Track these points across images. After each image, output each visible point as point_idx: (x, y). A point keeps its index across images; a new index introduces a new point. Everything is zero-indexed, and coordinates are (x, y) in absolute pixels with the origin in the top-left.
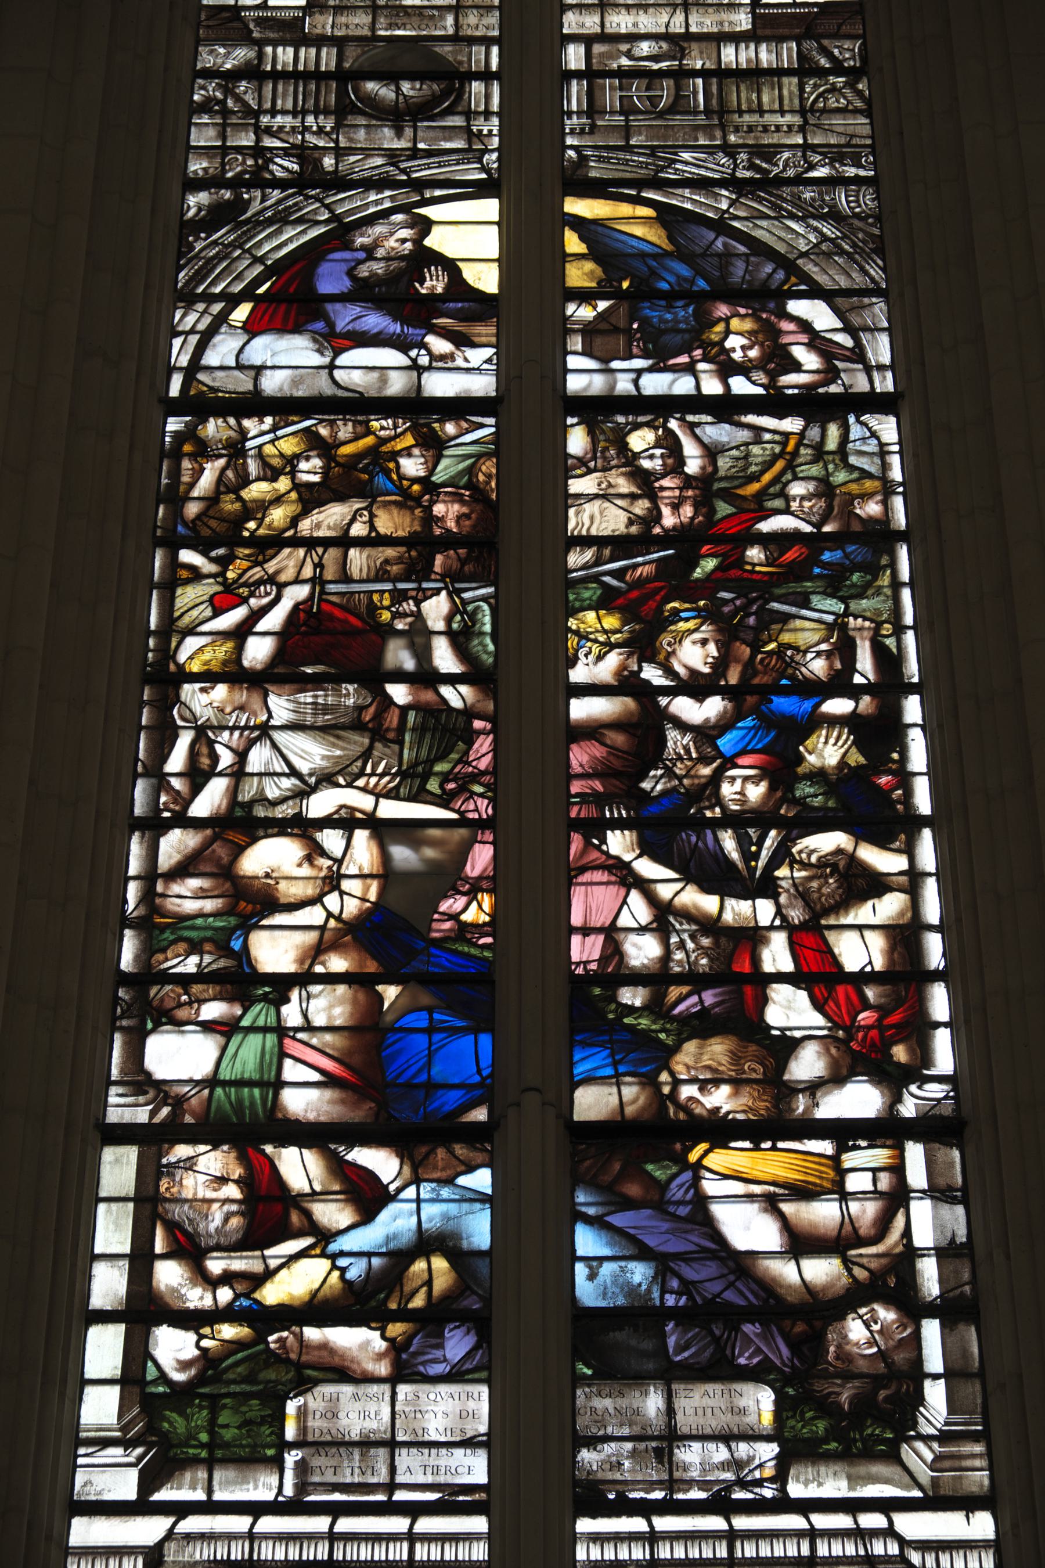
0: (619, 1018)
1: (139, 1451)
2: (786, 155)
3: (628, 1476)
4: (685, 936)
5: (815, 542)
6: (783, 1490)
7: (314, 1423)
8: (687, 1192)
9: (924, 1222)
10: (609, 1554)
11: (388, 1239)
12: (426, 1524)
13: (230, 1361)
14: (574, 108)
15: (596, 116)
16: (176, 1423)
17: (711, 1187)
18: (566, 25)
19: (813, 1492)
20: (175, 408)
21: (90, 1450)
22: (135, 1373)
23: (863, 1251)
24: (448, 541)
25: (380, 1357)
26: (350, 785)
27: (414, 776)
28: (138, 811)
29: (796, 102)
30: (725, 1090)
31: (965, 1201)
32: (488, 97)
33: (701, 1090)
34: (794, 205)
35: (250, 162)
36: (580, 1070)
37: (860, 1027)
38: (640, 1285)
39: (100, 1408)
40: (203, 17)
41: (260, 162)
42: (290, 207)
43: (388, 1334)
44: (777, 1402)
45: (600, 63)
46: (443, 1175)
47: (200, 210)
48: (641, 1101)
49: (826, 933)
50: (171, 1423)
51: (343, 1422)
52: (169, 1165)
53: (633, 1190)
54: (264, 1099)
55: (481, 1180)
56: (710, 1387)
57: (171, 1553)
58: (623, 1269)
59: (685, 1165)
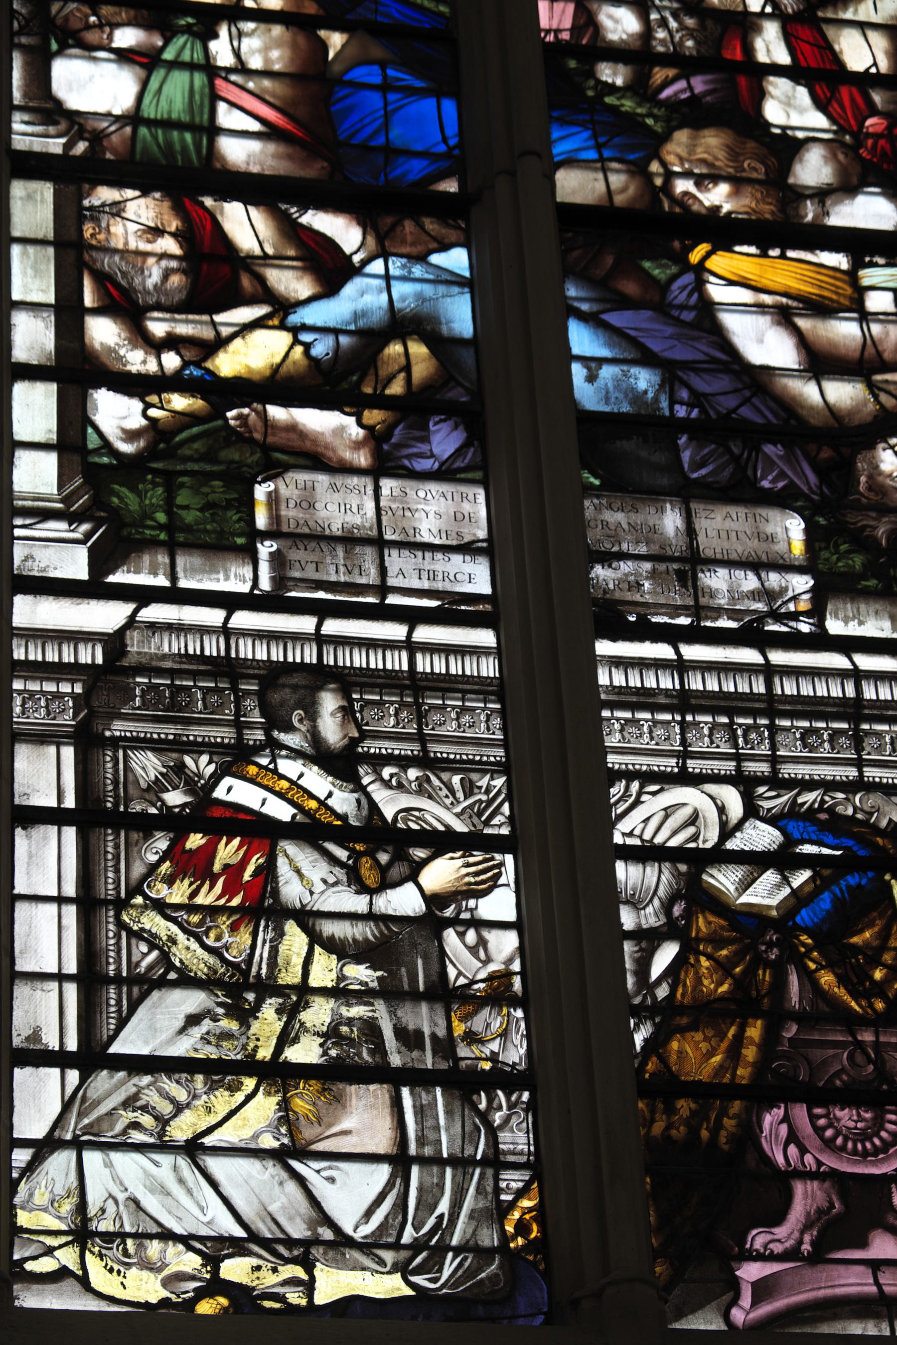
0: (600, 96)
3: (648, 598)
4: (667, 14)
6: (821, 624)
7: (289, 513)
8: (690, 295)
10: (635, 681)
11: (356, 316)
12: (425, 633)
13: (184, 435)
16: (127, 499)
17: (718, 292)
19: (853, 629)
21: (28, 521)
22: (73, 437)
25: (357, 445)
30: (724, 188)
33: (698, 184)
36: (560, 149)
37: (868, 135)
38: (646, 392)
44: (807, 531)
46: (414, 251)
48: (631, 191)
49: (824, 27)
50: (121, 499)
51: (322, 514)
52: (91, 208)
53: (630, 288)
54: (198, 145)
55: (457, 260)
56: (733, 510)
57: (135, 644)
58: (625, 374)
59: (686, 267)
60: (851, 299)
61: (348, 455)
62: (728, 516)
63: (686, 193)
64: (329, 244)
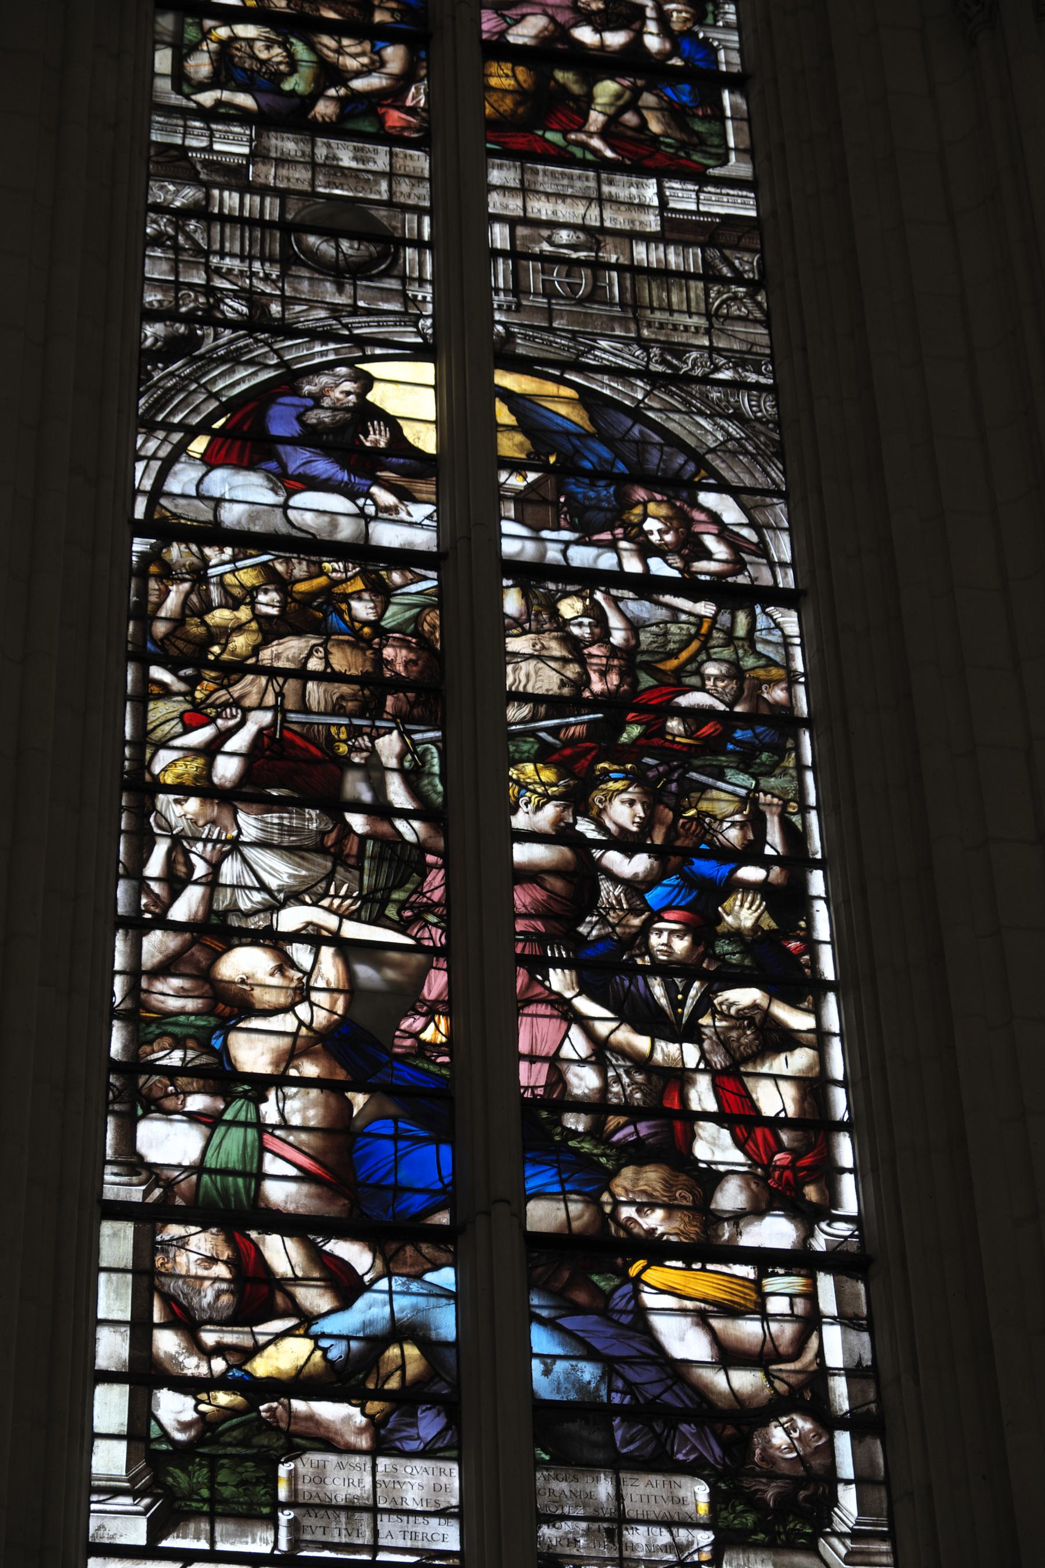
0: (565, 1141)
1: (146, 1501)
2: (694, 354)
3: (583, 1552)
4: (621, 1071)
5: (728, 719)
7: (304, 1487)
8: (628, 1302)
9: (834, 1345)
11: (365, 1325)
14: (501, 285)
17: (650, 1299)
18: (491, 205)
20: (141, 529)
23: (782, 1366)
24: (397, 684)
25: (361, 1431)
26: (315, 904)
27: (374, 901)
28: (121, 910)
29: (702, 305)
30: (659, 1213)
31: (870, 1329)
32: (421, 264)
33: (638, 1211)
34: (703, 403)
35: (202, 300)
36: (531, 1184)
37: (776, 1166)
38: (589, 1383)
39: (109, 1459)
40: (152, 152)
42: (241, 348)
43: (367, 1411)
44: (711, 1495)
45: (523, 245)
46: (412, 1270)
47: (156, 340)
48: (586, 1218)
49: (745, 1079)
51: (330, 1487)
53: (581, 1297)
54: (247, 1189)
55: (445, 1277)
58: (574, 1368)
59: (626, 1279)
60: (756, 1303)
61: (352, 1439)
62: (649, 1483)
63: (629, 1219)
64: (346, 1267)
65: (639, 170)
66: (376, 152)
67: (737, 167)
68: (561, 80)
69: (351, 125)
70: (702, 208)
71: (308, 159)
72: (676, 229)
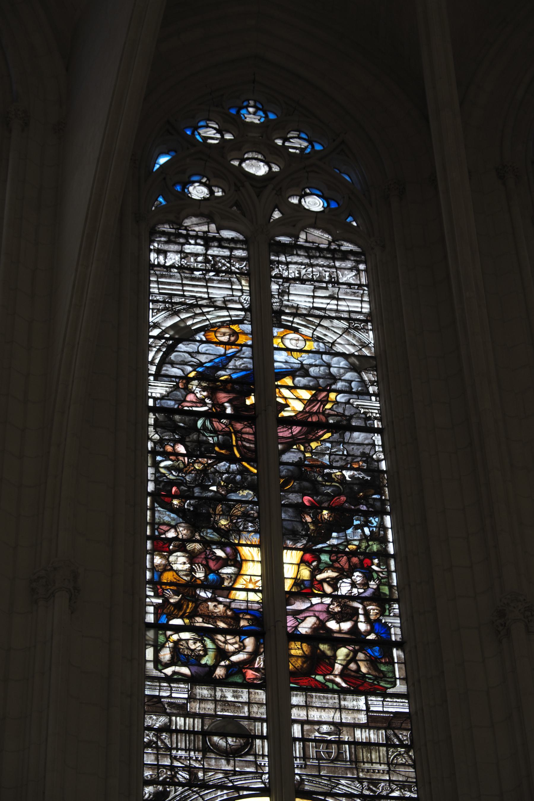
2: (382, 784)
15: (307, 760)
18: (293, 715)
29: (386, 759)
32: (263, 747)
35: (169, 773)
40: (146, 701)
41: (173, 773)
42: (186, 796)
45: (307, 734)
47: (150, 795)
65: (356, 692)
66: (242, 692)
67: (401, 687)
68: (322, 649)
69: (231, 680)
70: (385, 709)
71: (213, 698)
72: (374, 721)
